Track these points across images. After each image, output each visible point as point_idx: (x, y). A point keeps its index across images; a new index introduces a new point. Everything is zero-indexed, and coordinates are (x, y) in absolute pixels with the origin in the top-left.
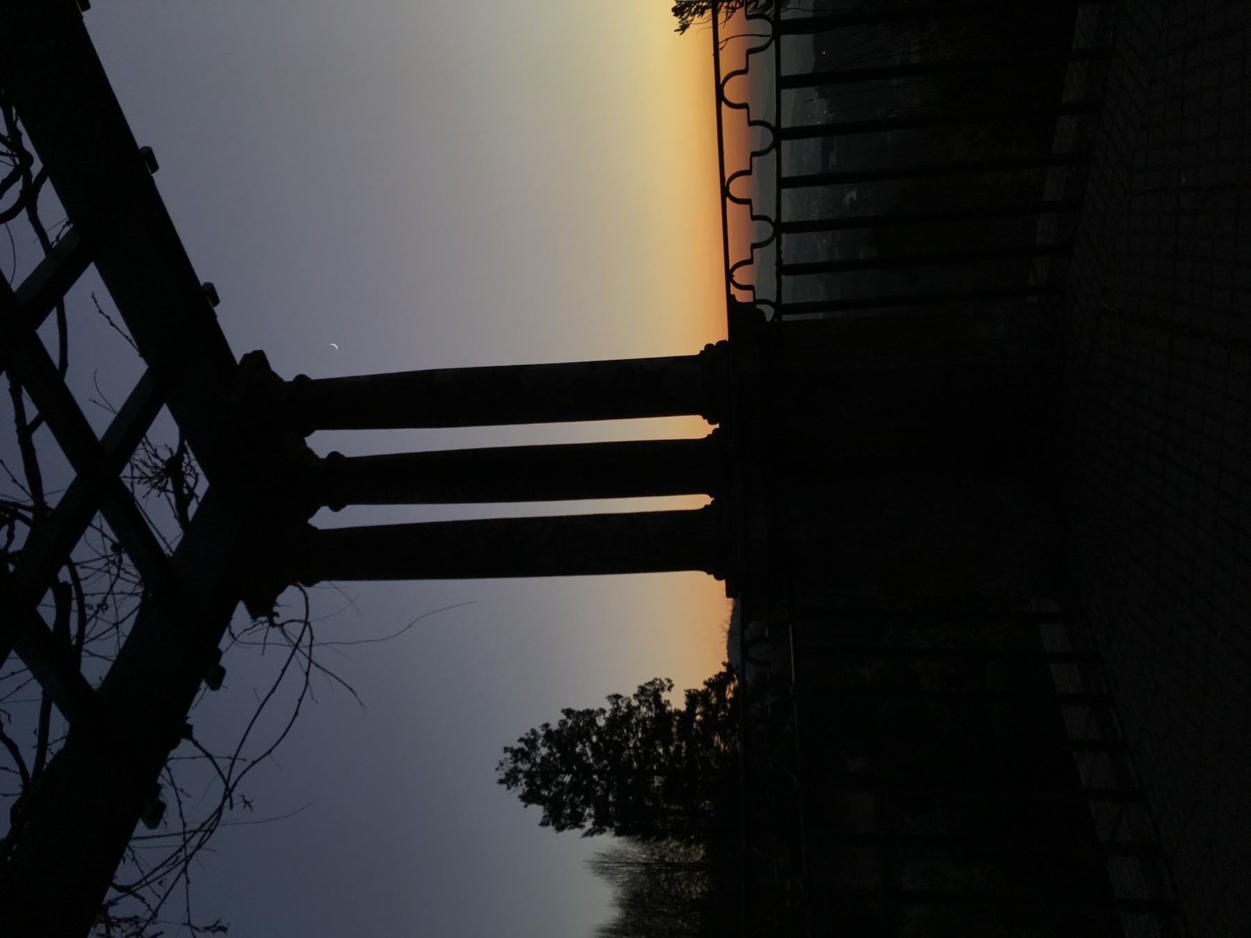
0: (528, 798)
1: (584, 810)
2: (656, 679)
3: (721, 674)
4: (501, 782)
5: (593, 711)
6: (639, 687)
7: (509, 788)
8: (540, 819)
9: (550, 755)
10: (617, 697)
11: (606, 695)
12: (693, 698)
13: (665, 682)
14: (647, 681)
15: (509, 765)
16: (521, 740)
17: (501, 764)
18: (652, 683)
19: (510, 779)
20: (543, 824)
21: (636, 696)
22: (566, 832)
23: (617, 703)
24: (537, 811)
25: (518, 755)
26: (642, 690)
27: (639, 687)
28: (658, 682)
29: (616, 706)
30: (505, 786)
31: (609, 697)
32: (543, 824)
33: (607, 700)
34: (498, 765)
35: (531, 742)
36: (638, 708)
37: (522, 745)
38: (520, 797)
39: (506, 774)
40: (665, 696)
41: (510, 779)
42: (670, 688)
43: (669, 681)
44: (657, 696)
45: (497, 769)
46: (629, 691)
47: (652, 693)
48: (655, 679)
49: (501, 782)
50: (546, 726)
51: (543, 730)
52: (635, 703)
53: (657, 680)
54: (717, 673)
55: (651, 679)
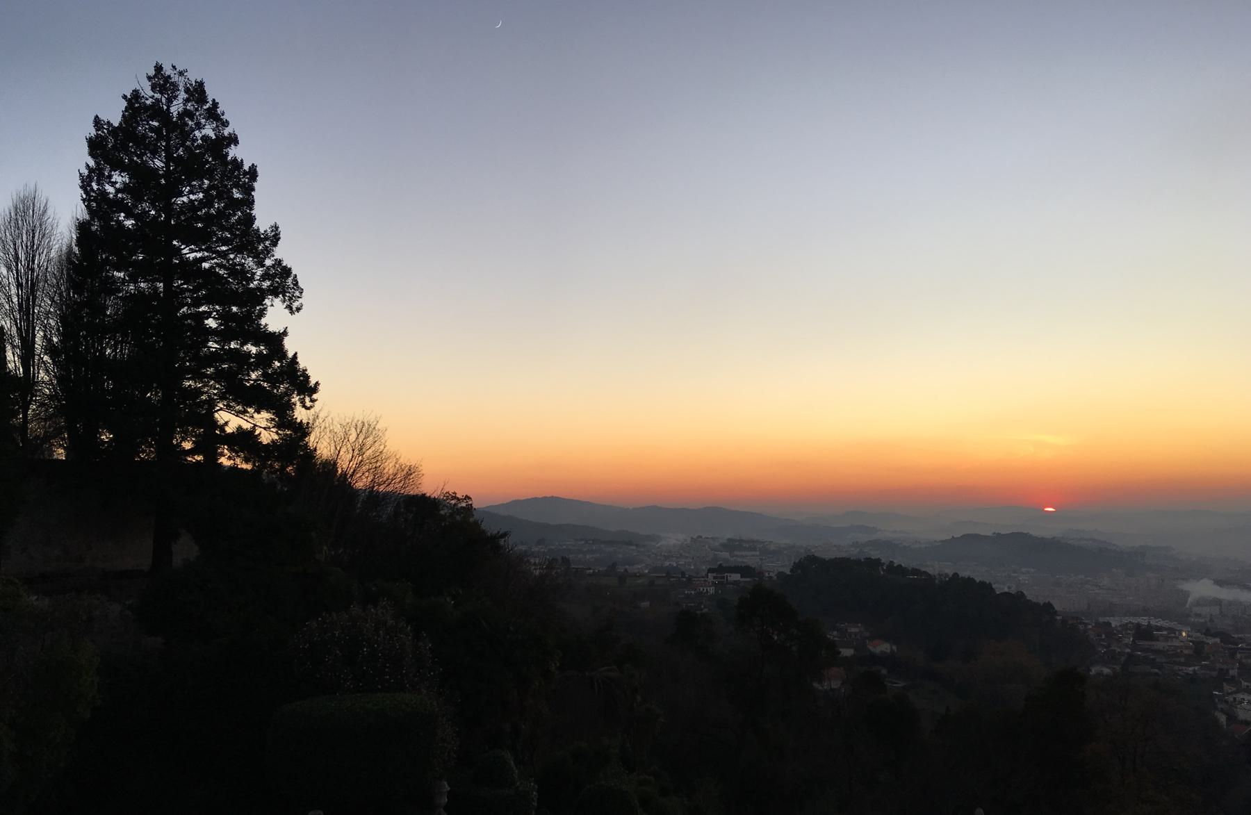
1: (146, 201)
3: (307, 377)
7: (149, 78)
8: (104, 117)
10: (275, 239)
11: (279, 224)
12: (275, 341)
13: (295, 305)
14: (299, 278)
16: (214, 100)
18: (296, 283)
19: (161, 81)
20: (97, 122)
21: (279, 262)
23: (266, 239)
24: (114, 116)
26: (287, 272)
27: (290, 269)
29: (262, 236)
31: (275, 228)
32: (97, 122)
33: (273, 224)
35: (213, 114)
36: (263, 266)
39: (169, 77)
41: (161, 81)
42: (289, 307)
43: (298, 309)
44: (274, 292)
45: (174, 67)
48: (302, 290)
51: (230, 134)
52: (268, 262)
54: (309, 372)
55: (300, 284)
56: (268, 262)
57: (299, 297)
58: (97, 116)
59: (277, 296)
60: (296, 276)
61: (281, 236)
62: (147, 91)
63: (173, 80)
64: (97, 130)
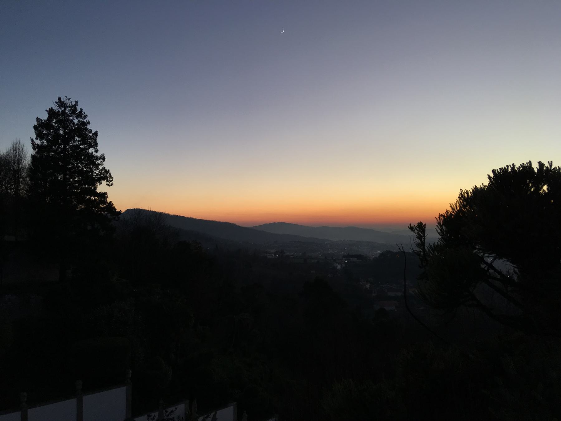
0: (51, 112)
2: (113, 178)
4: (60, 99)
5: (97, 147)
6: (109, 170)
7: (56, 102)
9: (74, 124)
10: (104, 159)
12: (104, 195)
13: (111, 183)
15: (68, 103)
16: (81, 110)
17: (69, 99)
18: (111, 176)
20: (38, 119)
21: (104, 168)
22: (34, 130)
23: (100, 159)
24: (44, 116)
25: (74, 108)
26: (107, 171)
27: (109, 170)
28: (111, 179)
29: (99, 158)
30: (57, 100)
32: (38, 119)
33: (102, 154)
34: (68, 97)
35: (80, 115)
36: (98, 169)
37: (79, 110)
38: (52, 108)
39: (64, 102)
40: (104, 182)
41: (61, 103)
43: (112, 185)
44: (104, 178)
46: (107, 165)
47: (106, 176)
48: (113, 178)
49: (60, 99)
50: (89, 123)
51: (87, 121)
52: (100, 167)
53: (112, 179)
55: (112, 176)
56: (100, 167)
57: (112, 180)
58: (37, 117)
59: (104, 180)
60: (110, 173)
61: (105, 158)
62: (55, 108)
63: (65, 103)
64: (37, 122)
